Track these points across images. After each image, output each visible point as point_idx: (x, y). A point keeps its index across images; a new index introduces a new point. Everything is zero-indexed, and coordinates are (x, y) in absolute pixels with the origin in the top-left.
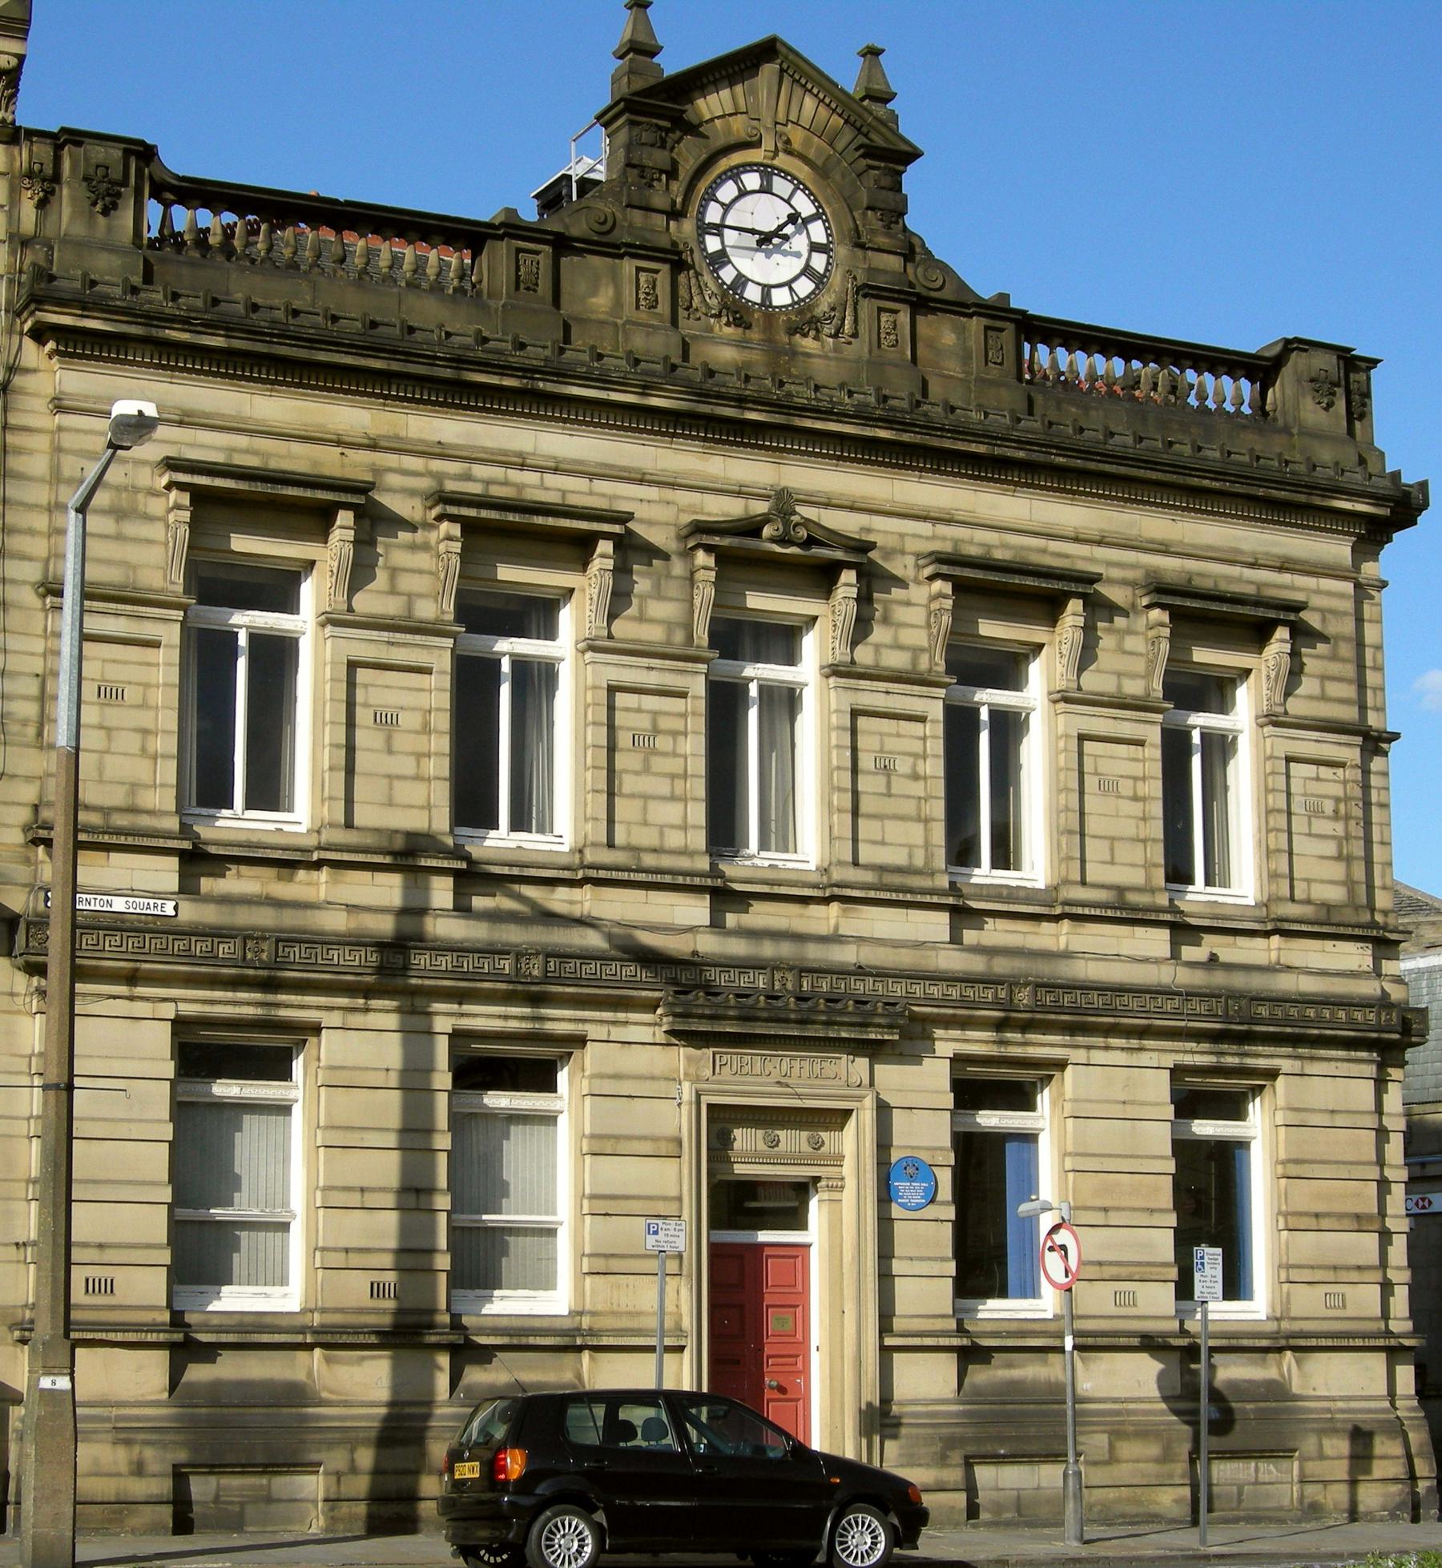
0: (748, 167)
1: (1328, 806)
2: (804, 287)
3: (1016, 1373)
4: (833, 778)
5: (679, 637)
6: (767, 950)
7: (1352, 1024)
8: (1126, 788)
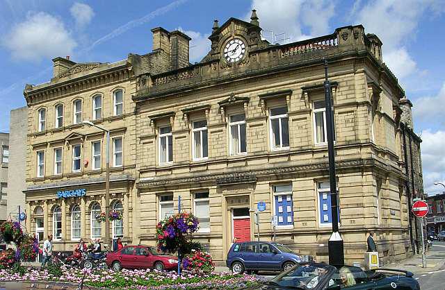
0: (230, 41)
1: (351, 121)
2: (241, 56)
3: (284, 239)
4: (264, 138)
5: (221, 121)
6: (235, 170)
7: (352, 165)
8: (304, 127)
